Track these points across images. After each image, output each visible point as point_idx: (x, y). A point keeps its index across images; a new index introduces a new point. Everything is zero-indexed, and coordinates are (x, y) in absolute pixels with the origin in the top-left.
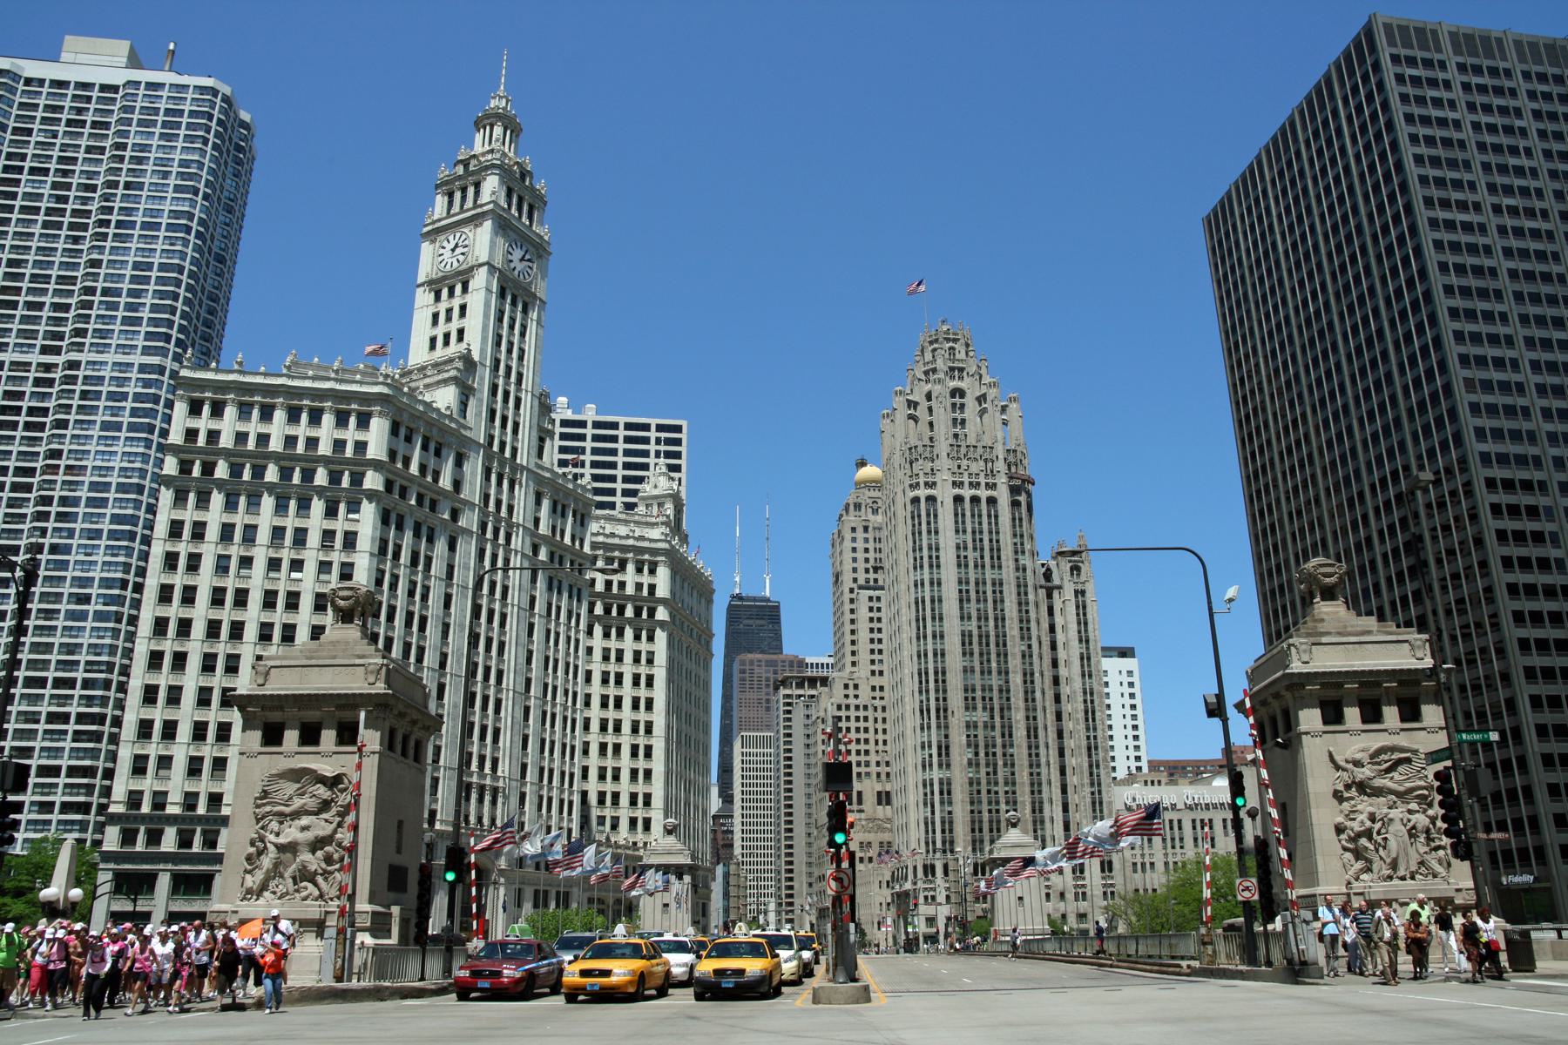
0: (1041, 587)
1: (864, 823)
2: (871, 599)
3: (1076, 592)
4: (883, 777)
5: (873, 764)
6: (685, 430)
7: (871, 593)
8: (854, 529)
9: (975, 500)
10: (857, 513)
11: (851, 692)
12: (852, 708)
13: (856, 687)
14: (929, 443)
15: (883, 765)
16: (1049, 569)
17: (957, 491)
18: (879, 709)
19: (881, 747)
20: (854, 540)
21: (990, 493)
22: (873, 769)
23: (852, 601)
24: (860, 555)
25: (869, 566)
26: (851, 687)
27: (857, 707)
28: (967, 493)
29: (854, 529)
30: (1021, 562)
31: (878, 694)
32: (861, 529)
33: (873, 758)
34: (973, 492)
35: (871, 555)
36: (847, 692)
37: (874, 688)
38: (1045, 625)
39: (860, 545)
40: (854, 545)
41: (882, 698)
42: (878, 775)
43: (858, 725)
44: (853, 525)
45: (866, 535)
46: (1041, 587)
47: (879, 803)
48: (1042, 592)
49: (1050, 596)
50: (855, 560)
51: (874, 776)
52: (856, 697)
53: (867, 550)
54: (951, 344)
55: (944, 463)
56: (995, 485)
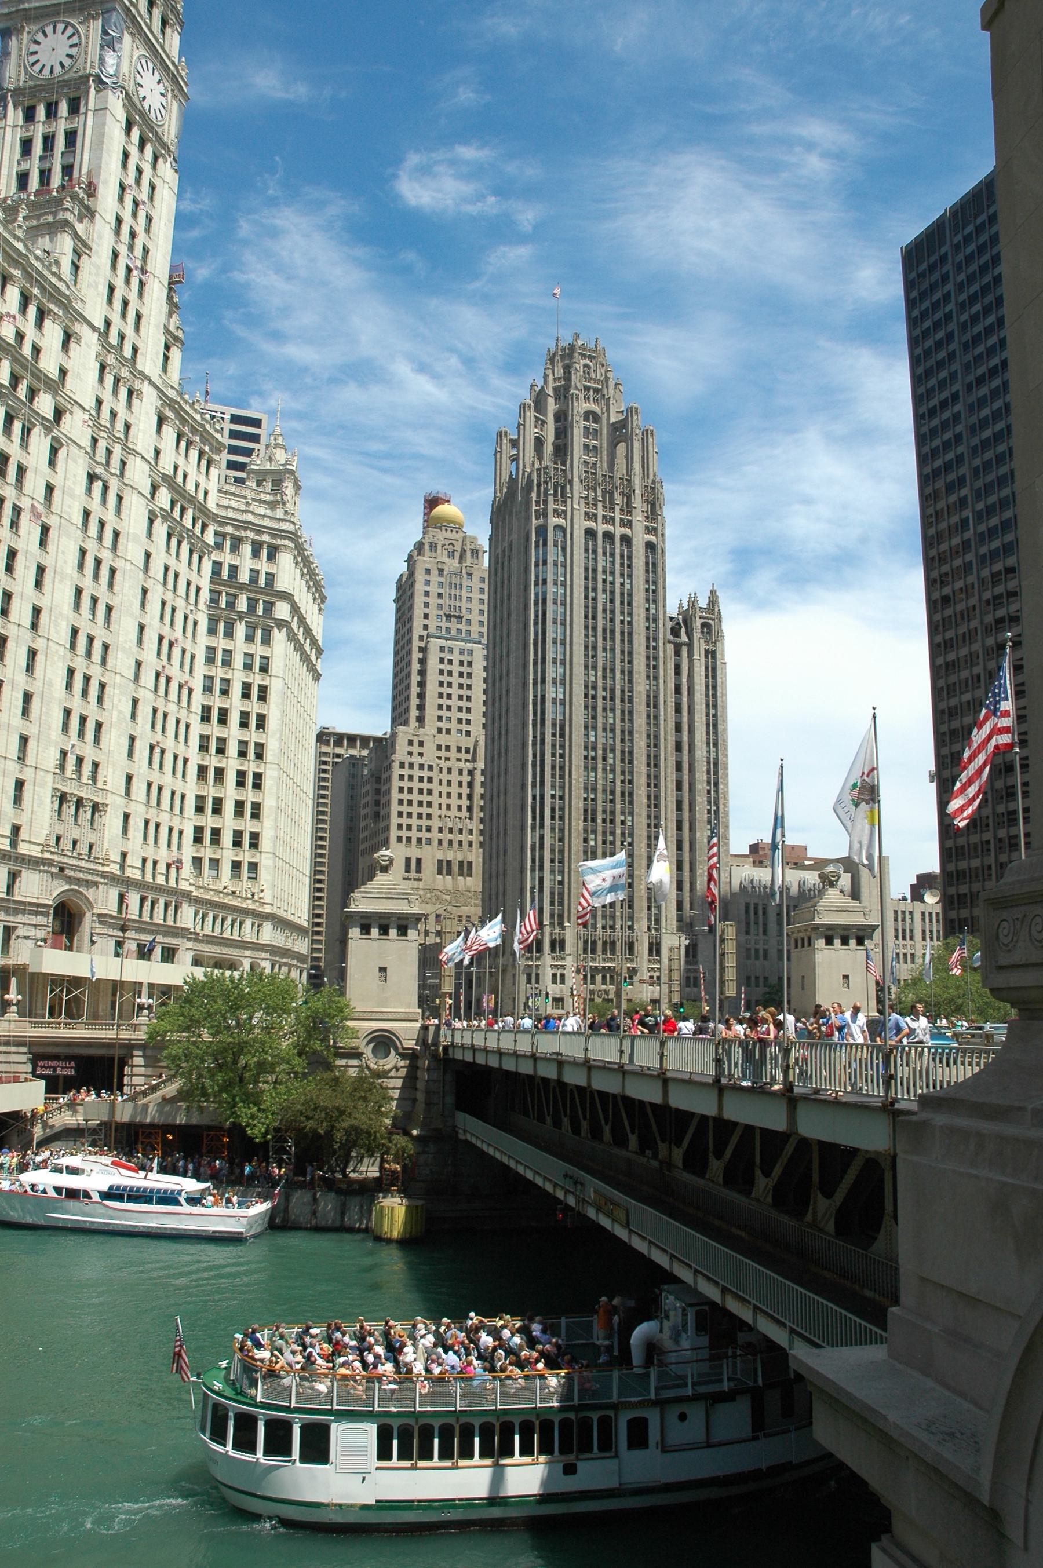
0: (669, 642)
1: (421, 892)
2: (442, 649)
3: (707, 652)
4: (445, 844)
5: (435, 829)
6: (264, 425)
7: (442, 643)
8: (428, 571)
9: (608, 536)
10: (434, 555)
11: (416, 749)
12: (416, 767)
13: (421, 744)
15: (446, 831)
16: (678, 624)
17: (591, 524)
18: (445, 771)
19: (444, 811)
20: (427, 583)
22: (435, 835)
24: (433, 600)
25: (441, 613)
26: (416, 743)
27: (421, 767)
28: (602, 528)
29: (428, 571)
30: (653, 611)
31: (443, 753)
32: (437, 572)
33: (435, 823)
35: (445, 601)
36: (410, 749)
37: (439, 748)
38: (671, 686)
40: (427, 588)
41: (447, 759)
42: (440, 841)
43: (421, 785)
44: (428, 566)
45: (442, 579)
46: (669, 642)
47: (440, 872)
48: (670, 647)
49: (678, 653)
51: (436, 843)
52: (421, 755)
54: (587, 361)
56: (630, 522)
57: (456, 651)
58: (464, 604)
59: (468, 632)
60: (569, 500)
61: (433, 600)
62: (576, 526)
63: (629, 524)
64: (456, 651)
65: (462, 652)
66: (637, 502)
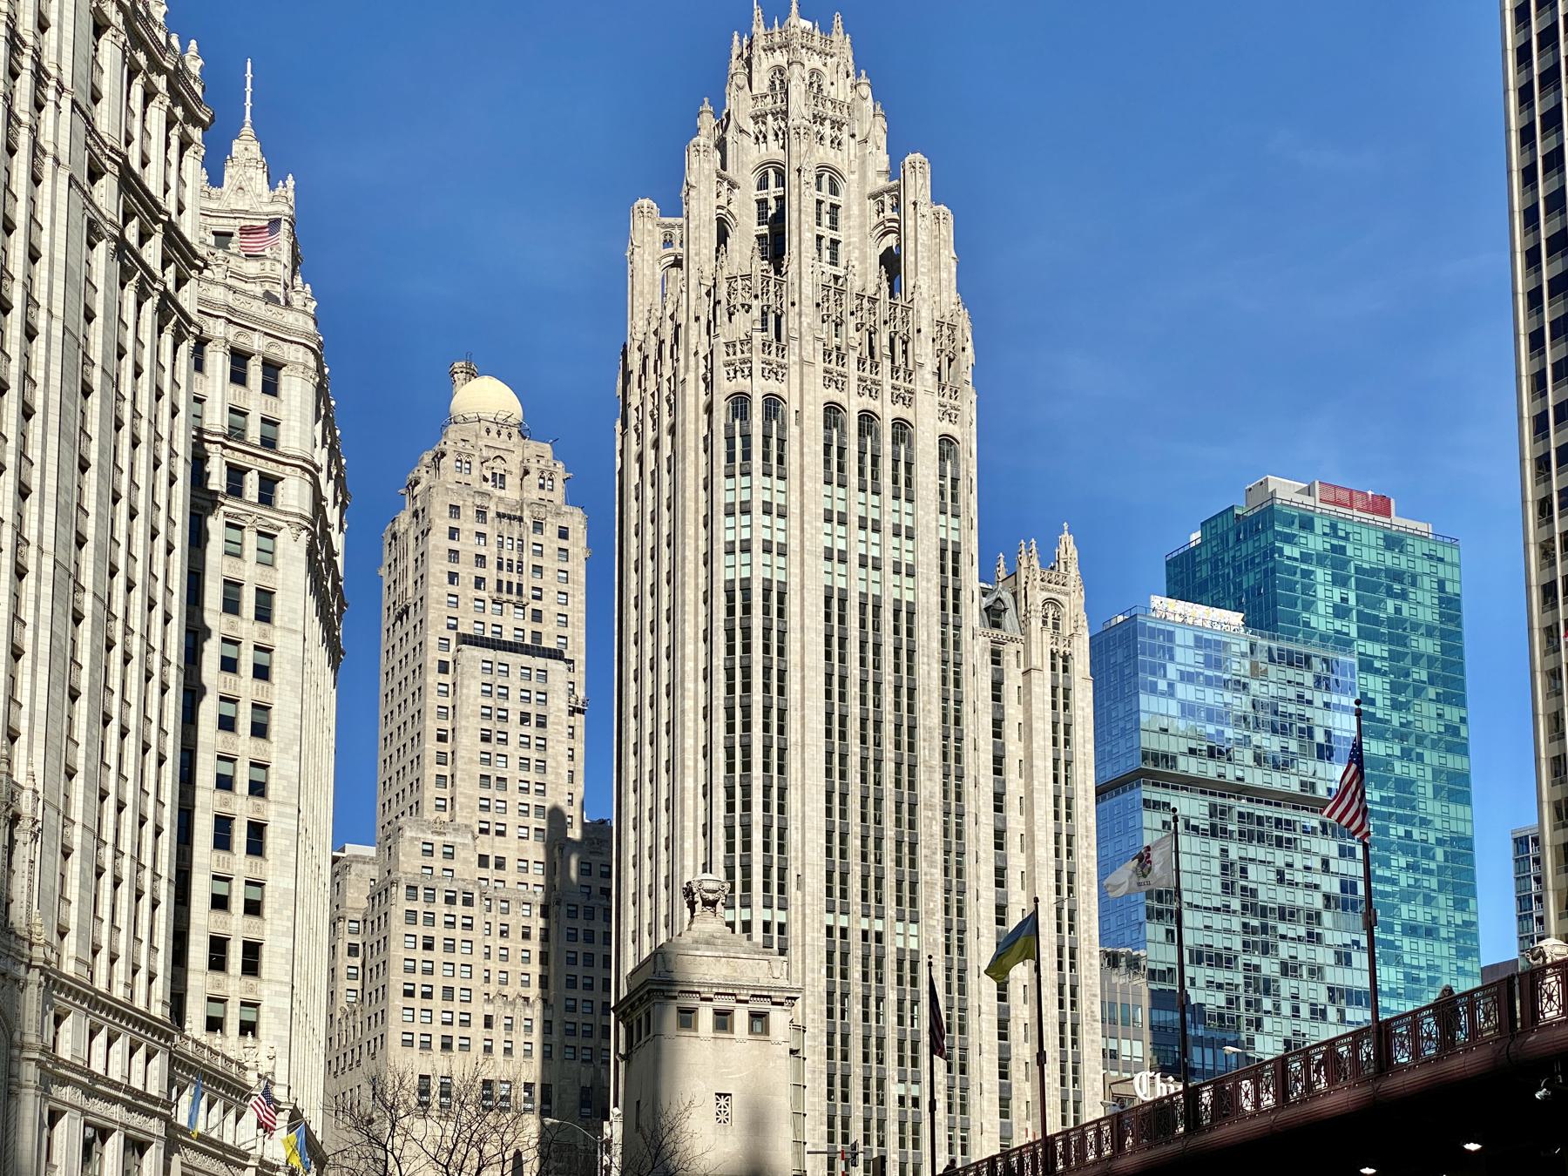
7: (489, 654)
8: (455, 510)
9: (867, 420)
20: (453, 533)
21: (900, 411)
23: (443, 667)
24: (467, 571)
28: (854, 404)
29: (455, 510)
34: (867, 403)
39: (467, 545)
40: (454, 545)
45: (481, 528)
50: (453, 577)
53: (481, 560)
57: (515, 673)
58: (529, 581)
59: (537, 636)
60: (794, 344)
61: (467, 571)
62: (806, 398)
63: (905, 397)
64: (515, 673)
65: (527, 673)
66: (924, 351)
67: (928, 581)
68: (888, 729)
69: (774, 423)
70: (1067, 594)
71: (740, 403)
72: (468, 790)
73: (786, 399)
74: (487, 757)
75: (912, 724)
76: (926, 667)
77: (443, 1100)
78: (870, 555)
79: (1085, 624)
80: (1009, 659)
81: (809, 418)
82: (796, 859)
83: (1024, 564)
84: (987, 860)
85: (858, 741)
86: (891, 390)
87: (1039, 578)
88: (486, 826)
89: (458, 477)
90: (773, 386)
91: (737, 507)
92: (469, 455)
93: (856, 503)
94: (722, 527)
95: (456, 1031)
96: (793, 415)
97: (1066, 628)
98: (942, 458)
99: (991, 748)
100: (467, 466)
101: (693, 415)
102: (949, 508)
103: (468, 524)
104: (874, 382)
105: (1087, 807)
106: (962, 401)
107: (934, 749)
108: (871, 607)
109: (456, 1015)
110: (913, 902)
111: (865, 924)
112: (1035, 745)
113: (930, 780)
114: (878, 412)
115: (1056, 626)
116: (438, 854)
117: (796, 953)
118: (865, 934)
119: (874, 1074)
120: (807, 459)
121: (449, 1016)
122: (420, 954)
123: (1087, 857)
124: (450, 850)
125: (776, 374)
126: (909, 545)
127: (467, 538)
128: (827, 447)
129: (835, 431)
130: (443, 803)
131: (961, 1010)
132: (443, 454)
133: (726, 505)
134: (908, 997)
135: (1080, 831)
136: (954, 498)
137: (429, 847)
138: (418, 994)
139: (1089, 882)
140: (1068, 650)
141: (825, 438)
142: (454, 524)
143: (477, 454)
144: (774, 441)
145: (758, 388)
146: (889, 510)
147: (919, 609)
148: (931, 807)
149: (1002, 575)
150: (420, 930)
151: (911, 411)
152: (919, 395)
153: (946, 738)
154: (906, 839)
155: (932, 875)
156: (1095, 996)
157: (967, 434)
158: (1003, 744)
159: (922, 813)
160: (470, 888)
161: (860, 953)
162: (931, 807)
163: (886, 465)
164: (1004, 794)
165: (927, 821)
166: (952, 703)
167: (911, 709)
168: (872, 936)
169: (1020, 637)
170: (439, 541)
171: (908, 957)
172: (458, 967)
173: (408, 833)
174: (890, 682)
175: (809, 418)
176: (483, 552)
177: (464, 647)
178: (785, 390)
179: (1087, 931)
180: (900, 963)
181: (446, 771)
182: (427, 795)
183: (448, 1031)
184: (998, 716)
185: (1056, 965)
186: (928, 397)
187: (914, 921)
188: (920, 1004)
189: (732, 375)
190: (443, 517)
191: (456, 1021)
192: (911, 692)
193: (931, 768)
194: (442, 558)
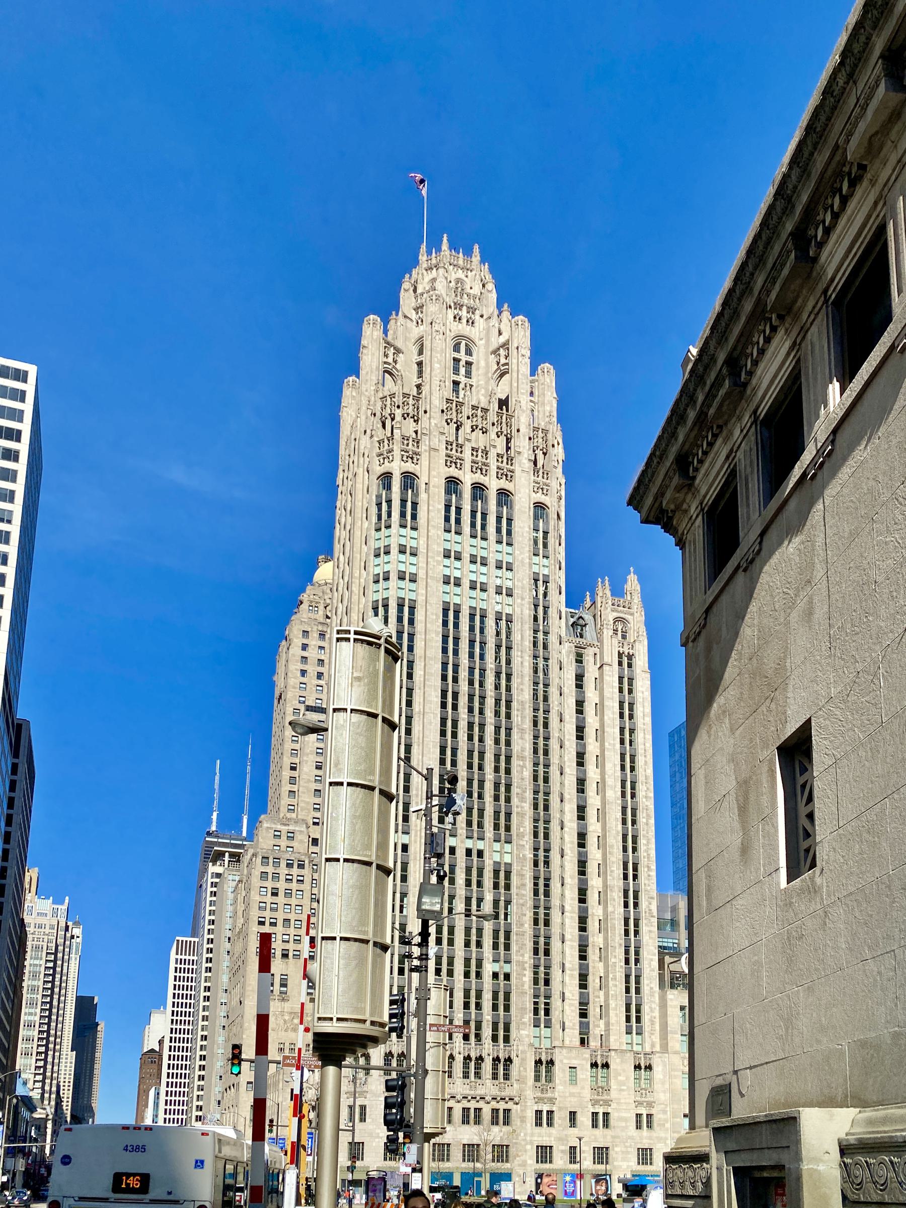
9: (478, 490)
14: (414, 392)
20: (305, 647)
21: (503, 484)
32: (316, 635)
34: (479, 478)
40: (305, 654)
45: (322, 644)
50: (303, 673)
55: (433, 421)
62: (433, 473)
67: (523, 599)
68: (490, 702)
69: (410, 491)
70: (632, 614)
71: (386, 478)
72: (306, 799)
73: (419, 475)
74: (320, 778)
75: (509, 699)
76: (519, 659)
77: (282, 989)
78: (479, 581)
79: (645, 634)
80: (588, 659)
81: (434, 486)
82: (417, 796)
83: (600, 594)
84: (570, 800)
85: (466, 711)
86: (496, 470)
87: (610, 603)
88: (317, 821)
89: (311, 615)
90: (409, 467)
91: (382, 550)
92: (317, 603)
93: (466, 544)
94: (372, 564)
95: (291, 946)
96: (423, 486)
97: (631, 637)
98: (536, 518)
99: (574, 720)
100: (316, 609)
101: (361, 496)
102: (541, 552)
103: (314, 641)
104: (484, 464)
105: (646, 762)
106: (551, 480)
107: (525, 717)
108: (478, 617)
109: (292, 936)
110: (508, 829)
111: (469, 844)
112: (606, 717)
113: (522, 739)
114: (486, 484)
115: (624, 637)
116: (284, 837)
117: (415, 866)
118: (469, 852)
119: (474, 955)
120: (431, 514)
121: (288, 937)
122: (269, 899)
123: (646, 797)
124: (292, 835)
125: (412, 458)
126: (509, 574)
127: (313, 649)
128: (448, 507)
129: (454, 496)
130: (293, 808)
131: (546, 908)
132: (302, 603)
133: (375, 549)
134: (502, 898)
135: (641, 778)
136: (545, 545)
137: (278, 833)
138: (267, 923)
139: (648, 816)
140: (631, 652)
141: (446, 500)
142: (305, 641)
143: (322, 602)
144: (409, 504)
145: (397, 467)
146: (492, 550)
147: (515, 618)
148: (522, 758)
149: (588, 606)
150: (270, 884)
151: (512, 484)
152: (518, 473)
153: (536, 710)
154: (503, 781)
155: (522, 807)
156: (652, 898)
157: (556, 503)
158: (584, 718)
159: (515, 762)
160: (303, 858)
161: (464, 865)
162: (522, 758)
163: (492, 520)
164: (584, 753)
165: (519, 768)
166: (541, 686)
167: (508, 689)
168: (475, 853)
169: (596, 643)
170: (296, 651)
171: (503, 869)
172: (293, 907)
173: (265, 825)
174: (491, 669)
175: (434, 486)
176: (322, 658)
177: (307, 713)
178: (421, 470)
179: (646, 851)
180: (496, 873)
181: (295, 788)
182: (283, 802)
183: (287, 946)
184: (580, 699)
185: (622, 876)
186: (525, 474)
187: (508, 842)
188: (512, 903)
189: (382, 461)
190: (299, 638)
191: (292, 940)
192: (509, 677)
193: (522, 731)
194: (297, 661)
